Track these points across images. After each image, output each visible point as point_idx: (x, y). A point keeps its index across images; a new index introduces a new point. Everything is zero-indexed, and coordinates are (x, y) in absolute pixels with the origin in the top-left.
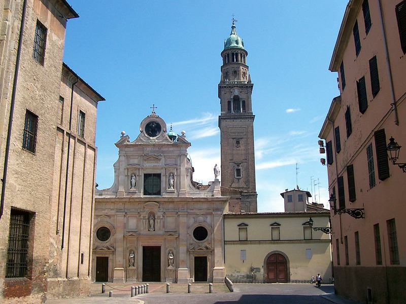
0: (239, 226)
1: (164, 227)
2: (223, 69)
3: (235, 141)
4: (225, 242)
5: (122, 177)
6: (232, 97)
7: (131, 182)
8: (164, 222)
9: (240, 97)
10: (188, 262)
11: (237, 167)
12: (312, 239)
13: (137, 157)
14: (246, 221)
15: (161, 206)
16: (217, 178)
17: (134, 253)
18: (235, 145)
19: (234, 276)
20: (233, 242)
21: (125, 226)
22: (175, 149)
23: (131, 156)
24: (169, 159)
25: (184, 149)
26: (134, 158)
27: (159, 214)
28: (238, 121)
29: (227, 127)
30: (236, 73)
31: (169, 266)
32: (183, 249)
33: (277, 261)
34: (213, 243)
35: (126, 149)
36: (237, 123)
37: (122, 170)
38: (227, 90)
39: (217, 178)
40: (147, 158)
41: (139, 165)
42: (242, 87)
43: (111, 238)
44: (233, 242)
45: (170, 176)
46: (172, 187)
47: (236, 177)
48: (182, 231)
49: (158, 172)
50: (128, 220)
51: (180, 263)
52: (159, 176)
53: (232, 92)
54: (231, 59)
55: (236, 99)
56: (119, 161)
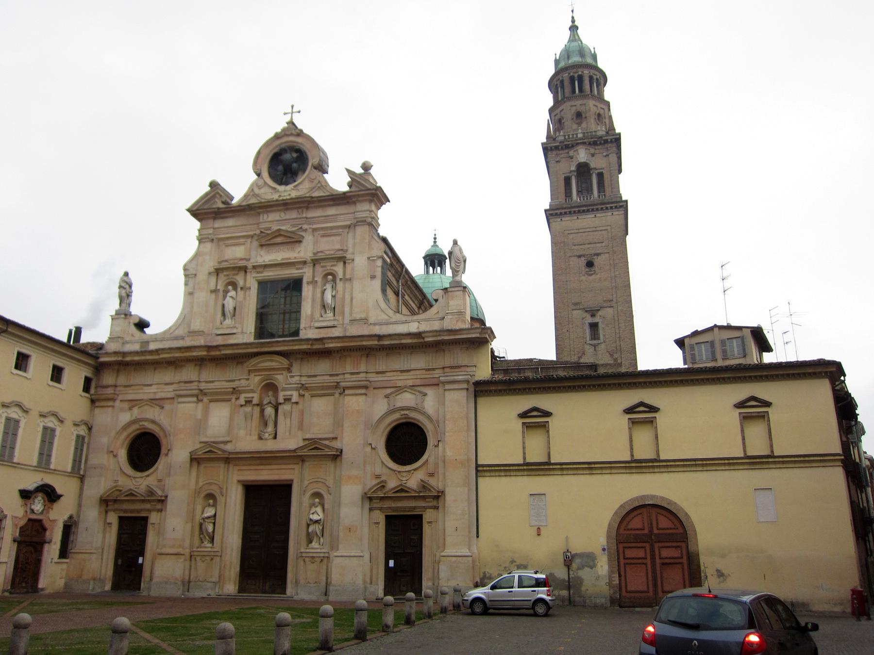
0: (523, 415)
1: (301, 427)
2: (553, 114)
3: (583, 261)
4: (481, 470)
5: (202, 296)
6: (573, 168)
7: (223, 306)
9: (592, 165)
10: (366, 530)
11: (590, 320)
13: (242, 240)
14: (544, 401)
16: (458, 278)
17: (214, 505)
18: (584, 269)
21: (201, 424)
23: (228, 238)
24: (325, 239)
25: (365, 206)
31: (310, 541)
33: (651, 531)
34: (441, 471)
35: (218, 224)
36: (588, 221)
37: (202, 276)
39: (458, 278)
40: (268, 240)
41: (248, 260)
42: (595, 143)
46: (330, 314)
49: (293, 273)
50: (206, 413)
51: (341, 534)
54: (568, 89)
55: (583, 170)
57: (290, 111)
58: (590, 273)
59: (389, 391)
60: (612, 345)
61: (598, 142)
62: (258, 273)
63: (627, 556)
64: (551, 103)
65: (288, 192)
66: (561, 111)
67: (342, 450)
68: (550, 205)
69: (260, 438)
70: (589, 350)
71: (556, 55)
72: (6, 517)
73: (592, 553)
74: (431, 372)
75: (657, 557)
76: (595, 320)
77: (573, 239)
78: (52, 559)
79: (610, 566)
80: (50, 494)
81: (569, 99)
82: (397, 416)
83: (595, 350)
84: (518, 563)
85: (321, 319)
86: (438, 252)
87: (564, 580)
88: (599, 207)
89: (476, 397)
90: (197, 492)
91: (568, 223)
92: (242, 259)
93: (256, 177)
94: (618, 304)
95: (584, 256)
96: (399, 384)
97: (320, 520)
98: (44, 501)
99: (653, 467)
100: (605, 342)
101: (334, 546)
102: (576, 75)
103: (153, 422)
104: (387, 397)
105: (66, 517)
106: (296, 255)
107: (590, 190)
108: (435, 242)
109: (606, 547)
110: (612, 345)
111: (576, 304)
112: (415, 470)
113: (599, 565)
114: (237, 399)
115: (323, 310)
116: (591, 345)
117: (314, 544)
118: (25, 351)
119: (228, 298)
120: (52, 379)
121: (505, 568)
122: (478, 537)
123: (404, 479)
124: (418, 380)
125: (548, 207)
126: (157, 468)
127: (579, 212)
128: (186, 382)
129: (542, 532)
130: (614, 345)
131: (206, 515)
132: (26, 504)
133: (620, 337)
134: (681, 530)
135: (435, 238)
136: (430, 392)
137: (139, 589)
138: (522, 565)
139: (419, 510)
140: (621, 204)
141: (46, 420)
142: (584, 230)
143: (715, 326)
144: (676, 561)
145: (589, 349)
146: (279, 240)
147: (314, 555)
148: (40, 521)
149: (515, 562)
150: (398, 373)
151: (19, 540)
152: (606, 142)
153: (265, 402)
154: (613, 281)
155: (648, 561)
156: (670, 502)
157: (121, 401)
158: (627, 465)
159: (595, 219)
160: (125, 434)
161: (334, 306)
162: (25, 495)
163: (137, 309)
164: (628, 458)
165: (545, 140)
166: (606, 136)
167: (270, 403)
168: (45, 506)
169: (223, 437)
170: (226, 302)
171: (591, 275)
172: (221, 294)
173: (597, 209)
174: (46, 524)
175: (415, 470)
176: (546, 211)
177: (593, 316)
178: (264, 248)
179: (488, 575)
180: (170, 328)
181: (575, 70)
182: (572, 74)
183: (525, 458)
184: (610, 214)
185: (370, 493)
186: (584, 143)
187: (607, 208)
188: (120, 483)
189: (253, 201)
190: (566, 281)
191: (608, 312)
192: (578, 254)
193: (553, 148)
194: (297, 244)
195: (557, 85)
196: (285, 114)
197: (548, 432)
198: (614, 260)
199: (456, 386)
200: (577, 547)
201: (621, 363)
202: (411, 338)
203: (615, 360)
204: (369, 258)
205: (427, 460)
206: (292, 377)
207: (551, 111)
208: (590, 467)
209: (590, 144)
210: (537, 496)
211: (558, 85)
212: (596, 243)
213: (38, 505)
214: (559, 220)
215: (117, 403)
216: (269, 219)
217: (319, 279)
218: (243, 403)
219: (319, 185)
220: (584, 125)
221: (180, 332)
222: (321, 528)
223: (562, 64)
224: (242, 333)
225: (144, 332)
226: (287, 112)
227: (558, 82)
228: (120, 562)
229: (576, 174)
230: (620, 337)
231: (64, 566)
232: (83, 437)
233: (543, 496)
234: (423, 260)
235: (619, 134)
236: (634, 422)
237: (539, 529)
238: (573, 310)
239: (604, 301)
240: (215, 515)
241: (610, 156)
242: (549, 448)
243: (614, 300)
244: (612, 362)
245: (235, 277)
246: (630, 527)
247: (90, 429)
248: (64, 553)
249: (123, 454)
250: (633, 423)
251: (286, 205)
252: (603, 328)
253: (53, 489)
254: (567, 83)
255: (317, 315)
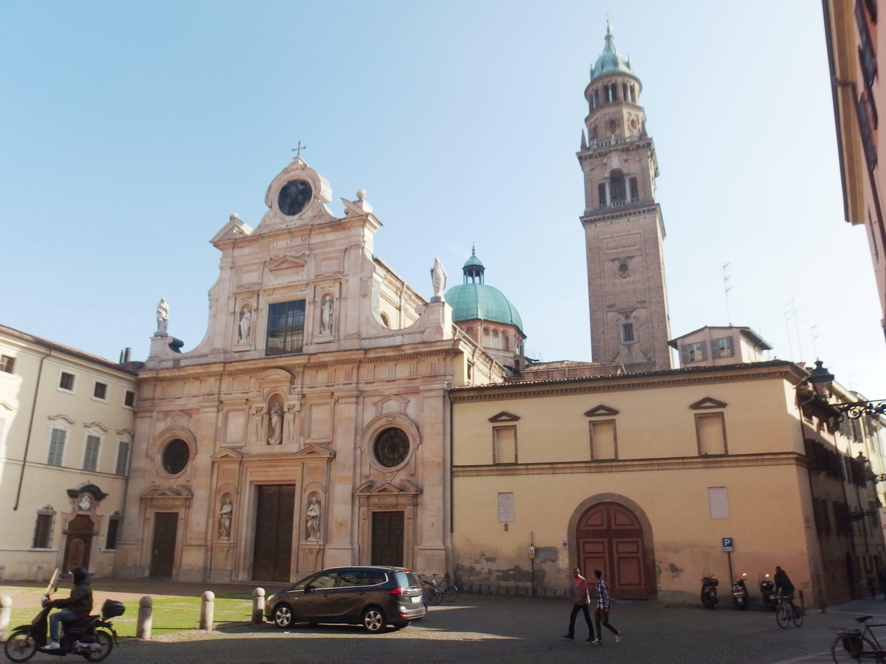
0: (494, 419)
2: (588, 124)
3: (616, 264)
5: (222, 317)
6: (607, 175)
7: (240, 326)
8: (303, 420)
9: (625, 171)
11: (623, 321)
12: (726, 455)
13: (256, 267)
15: (298, 381)
17: (231, 503)
19: (479, 573)
20: (476, 470)
21: (220, 432)
22: (339, 235)
23: (246, 265)
24: (325, 263)
26: (250, 271)
27: (292, 401)
28: (623, 221)
29: (598, 239)
30: (614, 124)
31: (308, 536)
32: (342, 490)
34: (420, 471)
37: (223, 301)
38: (596, 162)
40: (277, 264)
43: (188, 468)
44: (476, 470)
45: (324, 302)
46: (327, 332)
47: (623, 342)
48: (344, 444)
52: (299, 305)
53: (605, 165)
54: (601, 100)
55: (617, 178)
56: (220, 281)
57: (298, 147)
58: (624, 275)
59: (376, 399)
60: (646, 345)
61: (631, 148)
62: (269, 295)
63: (586, 551)
64: (587, 112)
65: (293, 221)
66: (595, 120)
67: (335, 454)
68: (585, 213)
69: (268, 443)
70: (624, 351)
71: (591, 65)
72: (55, 513)
73: (555, 548)
74: (413, 381)
75: (615, 552)
76: (630, 321)
77: (606, 244)
78: (100, 549)
79: (570, 560)
80: (96, 494)
81: (602, 107)
82: (383, 421)
83: (629, 350)
84: (487, 556)
85: (320, 335)
86: (476, 262)
87: (528, 572)
88: (632, 211)
89: (452, 404)
90: (218, 491)
91: (603, 228)
92: (255, 284)
93: (269, 209)
94: (652, 304)
95: (617, 259)
96: (386, 393)
97: (317, 516)
98: (91, 500)
99: (611, 466)
100: (638, 342)
101: (326, 540)
102: (610, 84)
103: (183, 429)
104: (375, 404)
105: (112, 514)
106: (300, 278)
107: (623, 195)
108: (473, 254)
109: (567, 542)
110: (646, 345)
111: (610, 306)
112: (398, 471)
113: (560, 558)
114: (250, 408)
115: (323, 328)
116: (625, 345)
117: (311, 539)
118: (69, 371)
119: (243, 319)
120: (96, 395)
121: (476, 560)
122: (452, 531)
123: (389, 479)
124: (402, 389)
125: (582, 215)
126: (186, 470)
127: (612, 217)
128: (208, 395)
129: (510, 527)
130: (648, 344)
131: (223, 512)
132: (74, 502)
133: (653, 337)
134: (638, 528)
135: (473, 250)
136: (413, 401)
137: (171, 576)
138: (492, 558)
139: (400, 507)
140: (653, 207)
141: (90, 430)
142: (618, 235)
143: (706, 327)
144: (634, 555)
145: (624, 349)
146: (285, 265)
147: (312, 547)
148: (87, 517)
149: (485, 555)
150: (385, 383)
151: (68, 532)
152: (638, 147)
153: (272, 412)
154: (647, 283)
155: (607, 555)
156: (628, 500)
157: (158, 412)
158: (587, 465)
159: (628, 223)
160: (161, 440)
161: (330, 324)
162: (73, 494)
163: (173, 332)
164: (589, 459)
165: (579, 150)
166: (638, 141)
167: (276, 412)
168: (92, 504)
169: (239, 442)
170: (241, 323)
171: (624, 278)
172: (238, 316)
173: (630, 214)
174: (94, 520)
175: (398, 471)
176: (581, 218)
177: (627, 317)
178: (274, 272)
179: (460, 567)
180: (198, 347)
181: (608, 79)
182: (605, 83)
183: (494, 460)
184: (642, 217)
185: (358, 492)
186: (617, 150)
187: (639, 212)
188: (156, 484)
189: (265, 231)
190: (601, 285)
191: (641, 313)
192: (612, 258)
193: (587, 157)
194: (301, 268)
195: (592, 95)
196: (293, 150)
197: (515, 435)
198: (646, 262)
199: (433, 394)
200: (541, 542)
201: (655, 362)
202: (393, 351)
203: (649, 359)
204: (361, 279)
205: (408, 463)
206: (296, 388)
207: (587, 120)
208: (553, 467)
209: (622, 150)
210: (506, 495)
211: (593, 95)
212: (629, 246)
213: (85, 503)
214: (594, 225)
215: (155, 414)
216: (278, 247)
217: (318, 299)
218: (255, 412)
219: (320, 214)
220: (617, 132)
221: (204, 351)
222: (318, 523)
223: (596, 75)
224: (255, 350)
225: (179, 352)
226: (294, 148)
227: (593, 93)
228: (157, 552)
229: (609, 180)
230: (653, 337)
231: (112, 555)
232: (127, 444)
233: (510, 494)
234: (463, 271)
235: (651, 139)
236: (593, 424)
237: (506, 525)
238: (607, 312)
239: (638, 302)
240: (231, 512)
241: (643, 160)
242: (516, 450)
243: (648, 301)
244: (645, 361)
245: (249, 300)
246: (589, 523)
247: (133, 437)
248: (111, 543)
249: (159, 458)
250: (594, 425)
251: (290, 232)
252: (637, 329)
253: (98, 490)
254: (601, 93)
255: (317, 331)
